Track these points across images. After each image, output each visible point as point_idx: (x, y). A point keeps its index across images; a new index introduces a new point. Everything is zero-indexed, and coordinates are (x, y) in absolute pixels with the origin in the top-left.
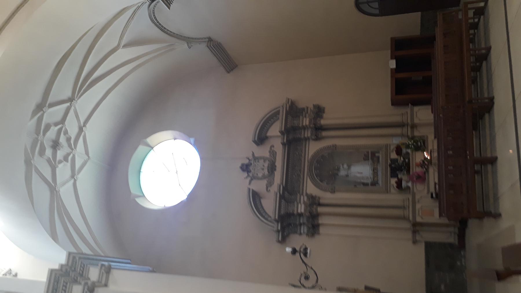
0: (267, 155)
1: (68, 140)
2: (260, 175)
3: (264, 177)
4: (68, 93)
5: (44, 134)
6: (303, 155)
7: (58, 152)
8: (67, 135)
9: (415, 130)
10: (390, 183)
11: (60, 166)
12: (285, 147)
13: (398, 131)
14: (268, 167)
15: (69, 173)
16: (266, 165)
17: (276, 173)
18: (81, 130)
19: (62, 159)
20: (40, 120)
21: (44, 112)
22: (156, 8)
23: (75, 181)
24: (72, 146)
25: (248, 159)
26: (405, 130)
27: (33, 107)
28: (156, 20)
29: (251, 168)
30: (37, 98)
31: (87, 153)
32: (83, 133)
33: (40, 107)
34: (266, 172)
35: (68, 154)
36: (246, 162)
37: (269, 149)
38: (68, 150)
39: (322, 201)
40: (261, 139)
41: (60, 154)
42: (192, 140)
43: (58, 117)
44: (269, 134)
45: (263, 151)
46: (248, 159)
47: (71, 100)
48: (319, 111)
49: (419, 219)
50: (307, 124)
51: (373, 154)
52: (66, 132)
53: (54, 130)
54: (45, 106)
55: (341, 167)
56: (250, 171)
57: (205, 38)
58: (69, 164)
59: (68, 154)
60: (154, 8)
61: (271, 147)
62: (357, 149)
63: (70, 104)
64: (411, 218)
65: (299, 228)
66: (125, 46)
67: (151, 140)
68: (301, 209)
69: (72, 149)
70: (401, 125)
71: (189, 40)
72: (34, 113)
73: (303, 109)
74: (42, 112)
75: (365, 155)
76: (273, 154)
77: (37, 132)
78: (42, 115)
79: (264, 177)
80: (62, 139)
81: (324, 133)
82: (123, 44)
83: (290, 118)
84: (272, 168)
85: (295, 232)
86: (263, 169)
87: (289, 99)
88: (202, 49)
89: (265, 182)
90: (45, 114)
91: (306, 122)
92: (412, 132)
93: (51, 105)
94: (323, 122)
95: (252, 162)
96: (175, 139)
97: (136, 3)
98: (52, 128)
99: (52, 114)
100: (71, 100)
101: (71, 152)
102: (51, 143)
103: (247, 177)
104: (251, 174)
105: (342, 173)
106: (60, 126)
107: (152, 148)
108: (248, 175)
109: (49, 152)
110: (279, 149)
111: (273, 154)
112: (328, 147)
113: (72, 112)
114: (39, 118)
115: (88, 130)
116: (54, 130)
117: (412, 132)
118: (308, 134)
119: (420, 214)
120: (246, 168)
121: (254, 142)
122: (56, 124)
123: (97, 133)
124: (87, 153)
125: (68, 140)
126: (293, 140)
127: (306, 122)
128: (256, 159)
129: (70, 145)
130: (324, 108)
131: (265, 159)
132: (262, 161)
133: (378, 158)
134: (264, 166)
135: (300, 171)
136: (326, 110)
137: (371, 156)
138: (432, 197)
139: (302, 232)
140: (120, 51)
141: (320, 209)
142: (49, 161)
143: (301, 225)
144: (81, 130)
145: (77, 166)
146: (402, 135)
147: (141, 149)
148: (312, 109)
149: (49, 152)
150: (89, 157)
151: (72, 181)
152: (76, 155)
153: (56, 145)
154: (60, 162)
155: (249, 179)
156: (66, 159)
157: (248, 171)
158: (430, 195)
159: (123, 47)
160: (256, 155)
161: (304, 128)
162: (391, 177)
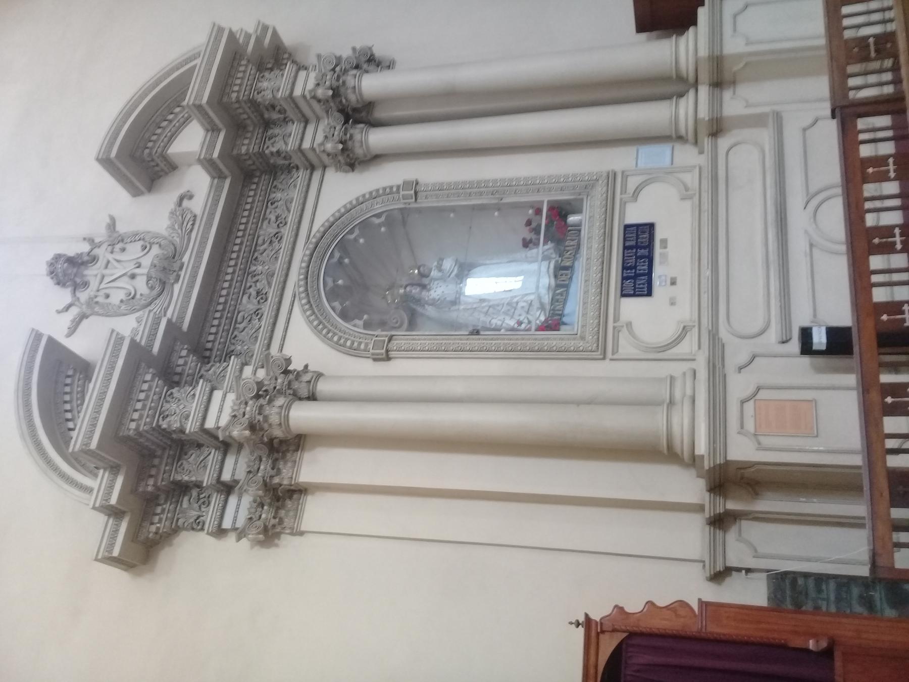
2: (117, 297)
6: (291, 218)
10: (616, 319)
12: (219, 189)
16: (147, 262)
29: (92, 273)
45: (152, 214)
46: (91, 241)
49: (741, 450)
51: (560, 212)
55: (434, 273)
56: (86, 284)
61: (181, 199)
64: (702, 448)
65: (216, 500)
81: (378, 139)
84: (166, 272)
85: (198, 525)
92: (716, 103)
95: (100, 252)
103: (67, 308)
104: (83, 296)
105: (438, 291)
112: (388, 192)
117: (716, 103)
119: (750, 426)
120: (69, 271)
128: (117, 240)
133: (578, 227)
138: (807, 348)
143: (228, 489)
155: (74, 311)
157: (78, 285)
158: (795, 345)
160: (122, 228)
162: (624, 295)
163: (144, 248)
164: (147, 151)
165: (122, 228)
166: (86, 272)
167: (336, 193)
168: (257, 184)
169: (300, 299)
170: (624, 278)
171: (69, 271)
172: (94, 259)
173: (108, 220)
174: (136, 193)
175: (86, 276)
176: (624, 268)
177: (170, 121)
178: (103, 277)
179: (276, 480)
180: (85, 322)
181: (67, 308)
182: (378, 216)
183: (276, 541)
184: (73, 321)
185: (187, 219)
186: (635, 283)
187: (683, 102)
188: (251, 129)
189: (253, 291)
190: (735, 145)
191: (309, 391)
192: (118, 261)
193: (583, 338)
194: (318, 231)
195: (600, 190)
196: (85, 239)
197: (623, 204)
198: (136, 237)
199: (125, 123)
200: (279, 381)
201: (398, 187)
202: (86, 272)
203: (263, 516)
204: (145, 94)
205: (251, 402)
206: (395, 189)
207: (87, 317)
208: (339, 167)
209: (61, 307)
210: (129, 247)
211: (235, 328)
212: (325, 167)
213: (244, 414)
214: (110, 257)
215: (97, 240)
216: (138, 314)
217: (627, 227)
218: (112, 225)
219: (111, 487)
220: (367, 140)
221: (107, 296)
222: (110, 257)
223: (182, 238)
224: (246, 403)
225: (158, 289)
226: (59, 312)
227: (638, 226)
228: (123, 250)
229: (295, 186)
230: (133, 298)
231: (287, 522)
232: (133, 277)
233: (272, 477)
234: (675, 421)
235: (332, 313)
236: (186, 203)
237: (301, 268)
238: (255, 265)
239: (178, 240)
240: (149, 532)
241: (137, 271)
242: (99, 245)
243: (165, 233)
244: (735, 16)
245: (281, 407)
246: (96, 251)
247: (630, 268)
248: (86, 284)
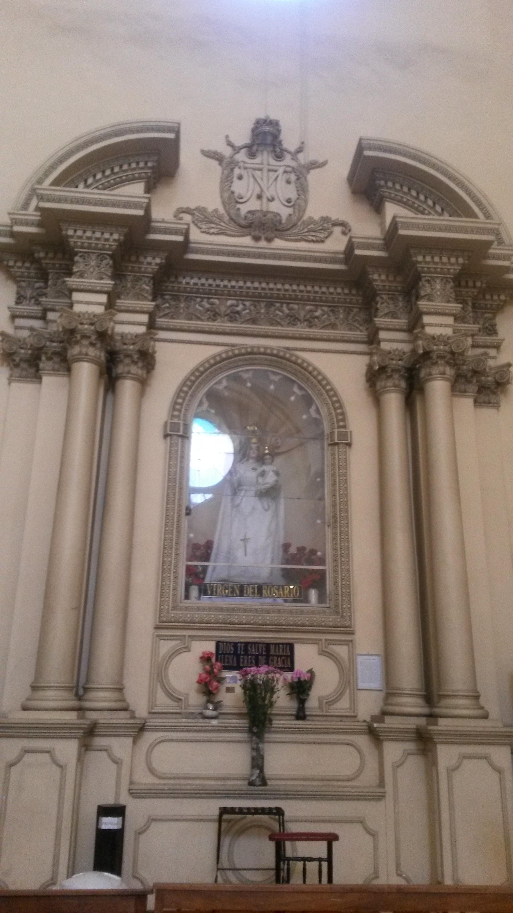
0: (315, 210)
3: (231, 200)
6: (315, 331)
9: (411, 746)
13: (409, 676)
14: (265, 214)
16: (275, 207)
17: (247, 241)
25: (300, 150)
26: (412, 704)
29: (265, 158)
34: (254, 205)
36: (289, 141)
37: (334, 217)
39: (127, 388)
44: (391, 210)
46: (300, 150)
48: (481, 385)
50: (429, 330)
51: (318, 581)
56: (252, 155)
61: (343, 224)
62: (339, 521)
65: (36, 309)
68: (89, 304)
70: (431, 691)
73: (492, 330)
75: (313, 552)
79: (231, 200)
81: (393, 402)
83: (454, 264)
84: (263, 226)
85: (20, 299)
86: (259, 197)
89: (213, 203)
91: (438, 325)
94: (438, 389)
95: (288, 160)
103: (230, 144)
104: (242, 156)
108: (236, 150)
118: (394, 342)
120: (266, 137)
126: (367, 288)
127: (438, 325)
130: (497, 406)
131: (298, 205)
132: (293, 196)
134: (271, 200)
135: (254, 321)
136: (487, 412)
137: (305, 572)
139: (20, 322)
141: (86, 373)
146: (390, 692)
148: (491, 363)
155: (227, 152)
157: (251, 150)
160: (313, 176)
161: (414, 325)
163: (289, 201)
164: (382, 183)
166: (265, 154)
167: (342, 369)
168: (350, 294)
169: (233, 351)
170: (235, 644)
171: (266, 137)
172: (279, 157)
173: (321, 160)
174: (351, 179)
175: (262, 154)
176: (246, 644)
177: (417, 198)
178: (260, 170)
179: (43, 358)
180: (215, 163)
181: (230, 144)
182: (318, 411)
183: (5, 364)
184: (216, 153)
185: (318, 234)
186: (230, 654)
187: (420, 701)
188: (399, 279)
189: (240, 308)
190: (359, 751)
191: (121, 374)
192: (276, 179)
193: (174, 608)
194: (297, 357)
195: (331, 619)
197: (315, 642)
198: (302, 189)
199: (405, 155)
200: (132, 347)
201: (344, 427)
202: (265, 154)
203: (23, 351)
204: (437, 169)
205: (93, 328)
206: (341, 424)
207: (220, 164)
208: (370, 367)
209: (232, 139)
210: (292, 187)
211: (202, 298)
212: (370, 354)
213: (82, 324)
216: (222, 210)
217: (291, 647)
218: (314, 165)
219: (26, 223)
220: (389, 392)
221: (240, 178)
222: (281, 170)
223: (298, 234)
224: (92, 324)
225: (243, 222)
226: (227, 137)
227: (291, 657)
229: (350, 330)
230: (237, 202)
231: (17, 371)
232: (259, 197)
233: (46, 353)
234: (50, 693)
235: (213, 383)
236: (337, 230)
237: (259, 348)
238: (266, 306)
240: (8, 261)
241: (265, 200)
243: (305, 217)
244: (486, 757)
245: (87, 354)
246: (288, 157)
247: (246, 650)
248: (252, 155)
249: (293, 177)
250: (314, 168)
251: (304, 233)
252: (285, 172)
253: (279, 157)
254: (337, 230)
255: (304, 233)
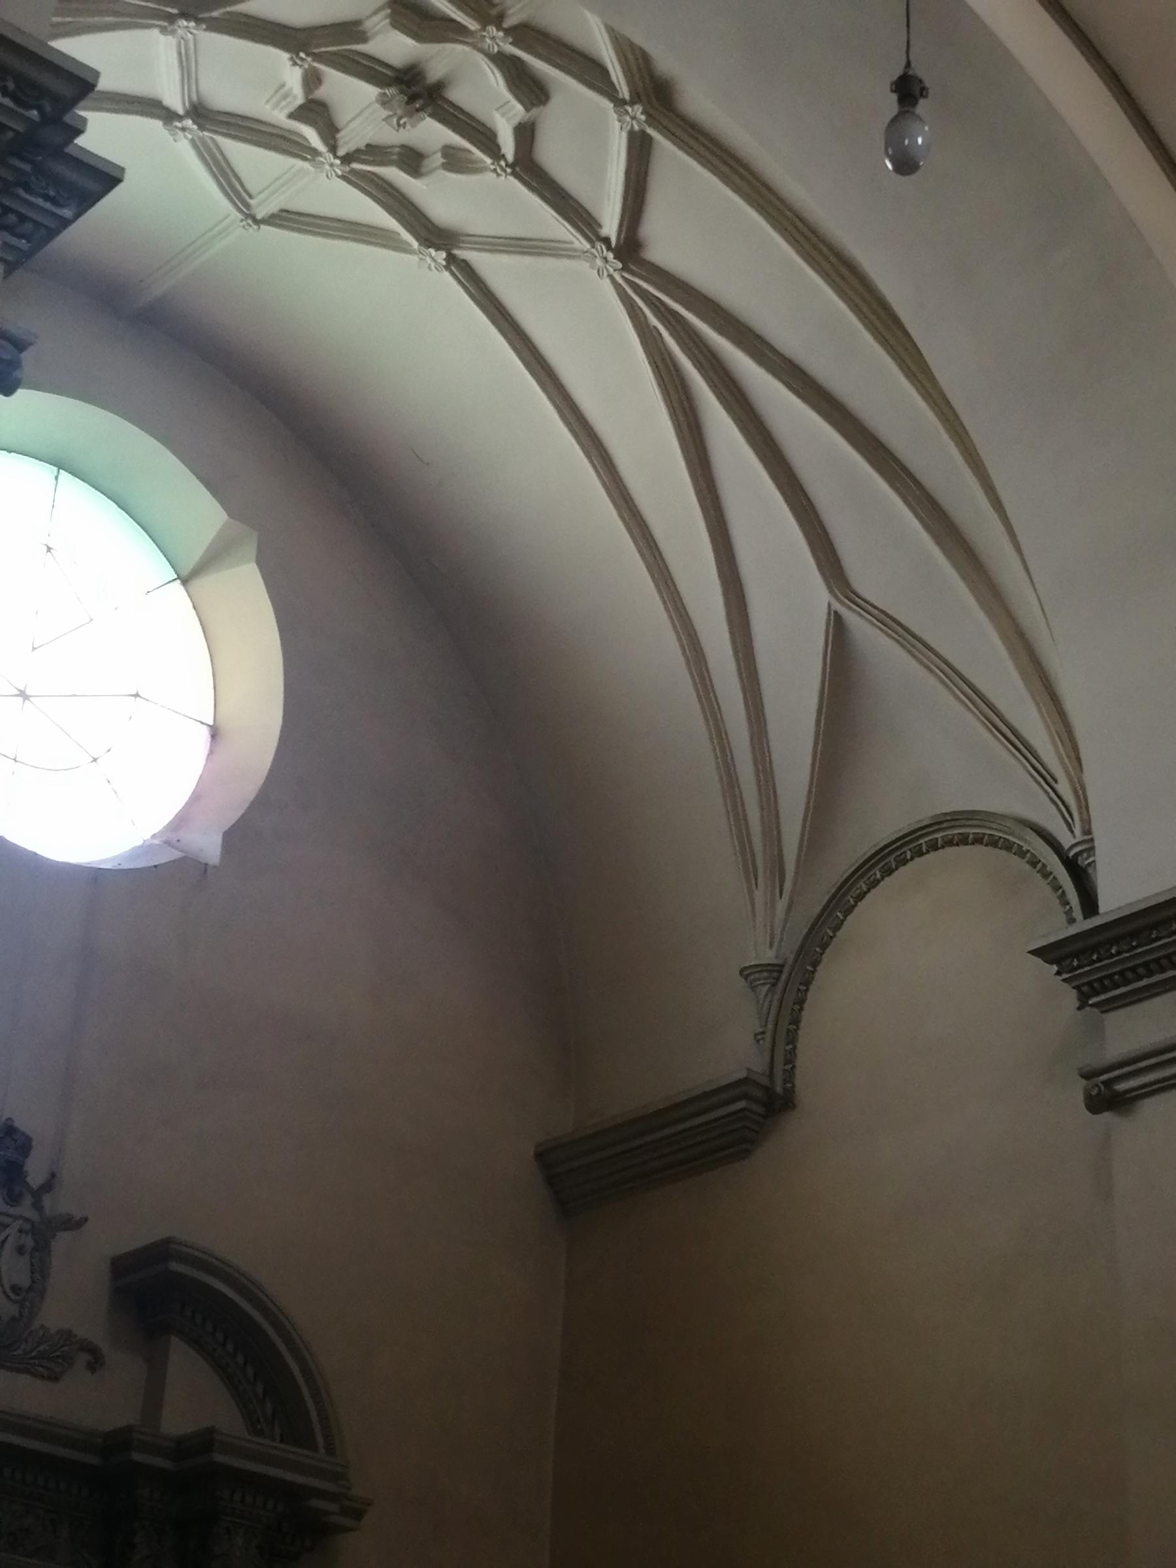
1: (412, 160)
4: (665, 244)
5: (502, 61)
7: (371, 91)
8: (438, 159)
11: (293, 77)
15: (224, 95)
18: (434, 235)
19: (321, 93)
20: (590, 71)
21: (619, 103)
22: (1023, 865)
23: (168, 116)
24: (363, 165)
27: (666, 62)
28: (949, 843)
30: (699, 100)
31: (285, 219)
32: (415, 244)
33: (655, 94)
35: (330, 132)
36: (35, 1171)
38: (352, 138)
40: (163, 1293)
41: (357, 102)
42: (208, 844)
43: (554, 154)
45: (75, 1298)
47: (629, 250)
52: (454, 161)
53: (504, 115)
54: (651, 120)
57: (790, 1075)
58: (279, 116)
59: (330, 132)
60: (1021, 853)
63: (606, 241)
66: (837, 628)
67: (245, 589)
69: (347, 159)
71: (789, 984)
72: (638, 63)
74: (624, 92)
76: (54, 1358)
77: (528, 34)
78: (605, 87)
80: (431, 133)
82: (851, 618)
87: (358, 1515)
88: (730, 1048)
90: (608, 105)
93: (640, 152)
95: (25, 1209)
96: (215, 733)
97: (1091, 776)
98: (518, 110)
99: (591, 140)
100: (629, 250)
101: (333, 149)
102: (435, 72)
106: (508, 144)
107: (185, 581)
109: (394, 45)
110: (92, 1402)
111: (54, 1358)
113: (547, 222)
114: (604, 71)
115: (423, 274)
116: (504, 115)
121: (162, 1251)
122: (526, 134)
123: (383, 316)
124: (285, 219)
125: (412, 160)
128: (42, 1235)
129: (374, 152)
132: (24, 1281)
140: (820, 596)
142: (350, 30)
144: (434, 235)
145: (241, 154)
147: (203, 515)
149: (394, 45)
150: (257, 222)
151: (174, 100)
152: (306, 165)
153: (416, 90)
154: (312, 80)
156: (315, 111)
159: (838, 618)
163: (15, 1289)
165: (62, 1242)
172: (13, 1199)
173: (78, 1215)
177: (224, 1345)
196: (53, 1175)
198: (40, 1270)
214: (12, 1231)
215: (47, 1200)
228: (20, 1250)
239: (20, 1352)
242: (38, 1206)
243: (36, 1324)
246: (28, 1200)
249: (29, 1241)
250: (65, 1230)
251: (32, 1358)
252: (21, 1231)
253: (13, 1199)
254: (83, 1358)
255: (32, 1358)
